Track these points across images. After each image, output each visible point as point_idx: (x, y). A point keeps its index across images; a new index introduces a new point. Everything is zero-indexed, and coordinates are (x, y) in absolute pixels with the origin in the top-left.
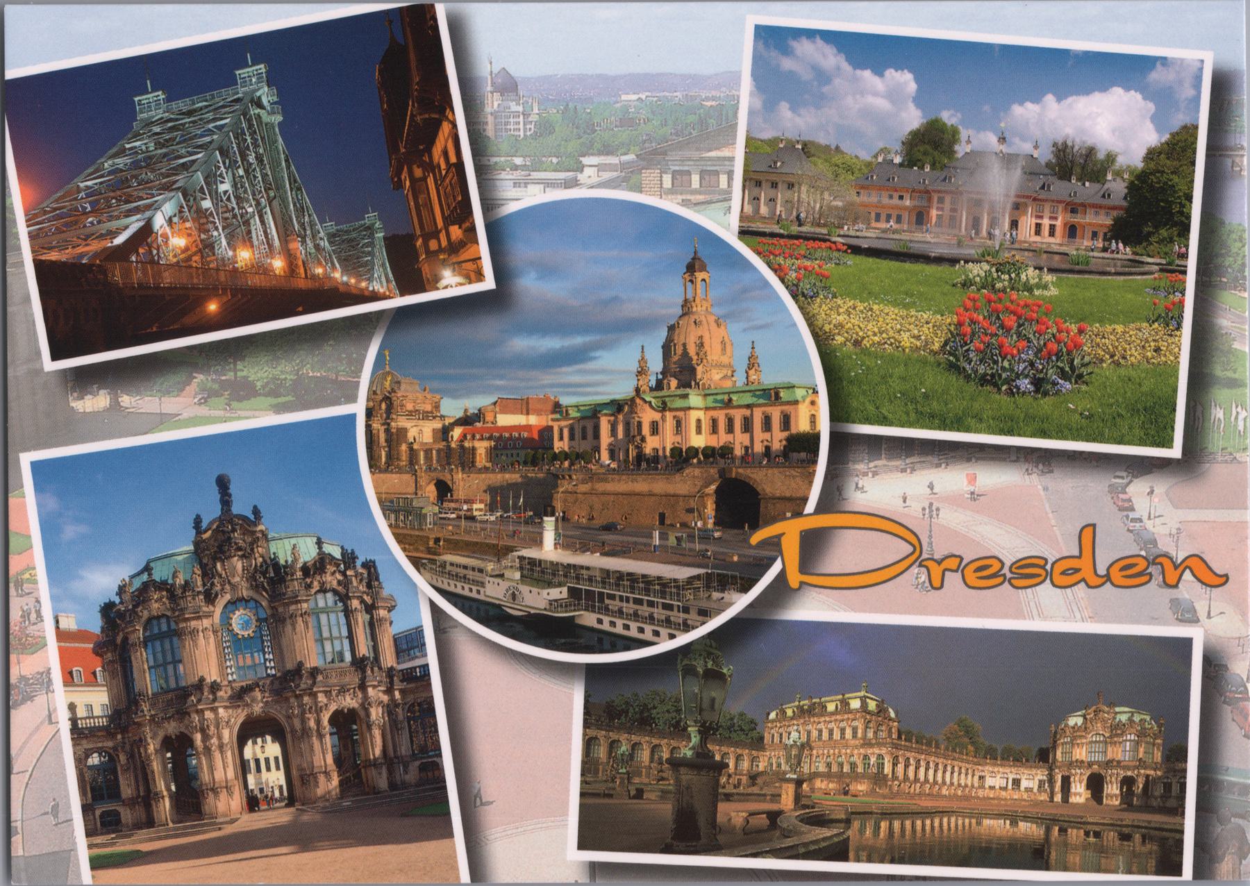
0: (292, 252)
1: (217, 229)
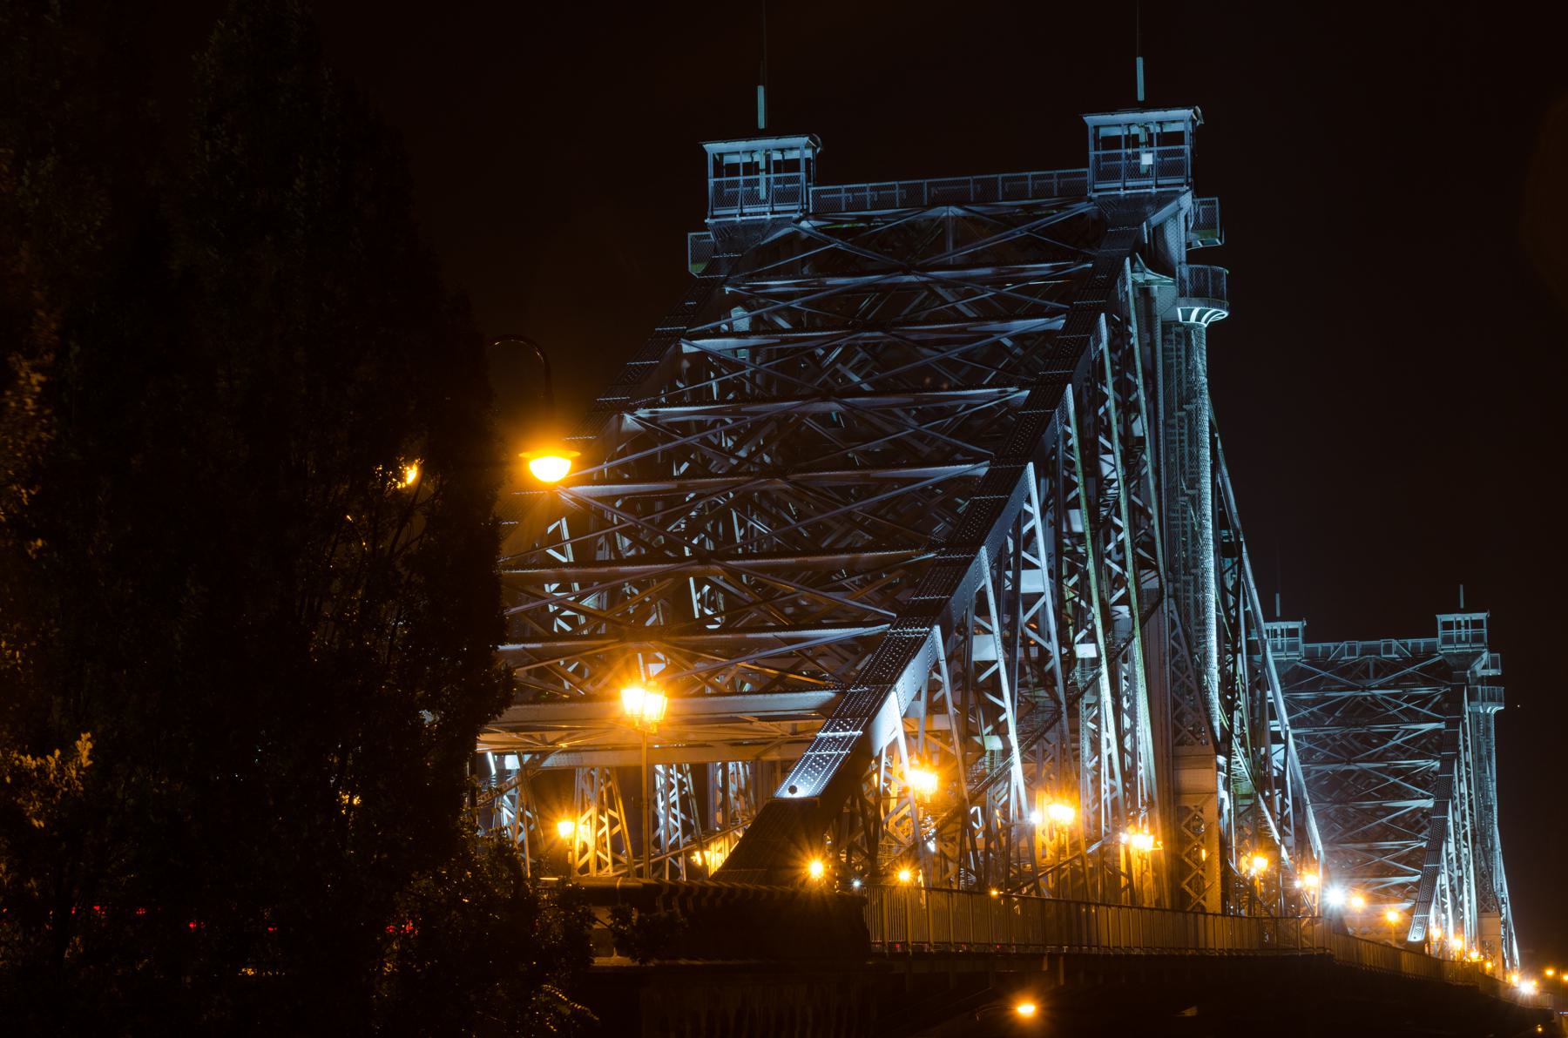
0: (1189, 802)
1: (1001, 730)
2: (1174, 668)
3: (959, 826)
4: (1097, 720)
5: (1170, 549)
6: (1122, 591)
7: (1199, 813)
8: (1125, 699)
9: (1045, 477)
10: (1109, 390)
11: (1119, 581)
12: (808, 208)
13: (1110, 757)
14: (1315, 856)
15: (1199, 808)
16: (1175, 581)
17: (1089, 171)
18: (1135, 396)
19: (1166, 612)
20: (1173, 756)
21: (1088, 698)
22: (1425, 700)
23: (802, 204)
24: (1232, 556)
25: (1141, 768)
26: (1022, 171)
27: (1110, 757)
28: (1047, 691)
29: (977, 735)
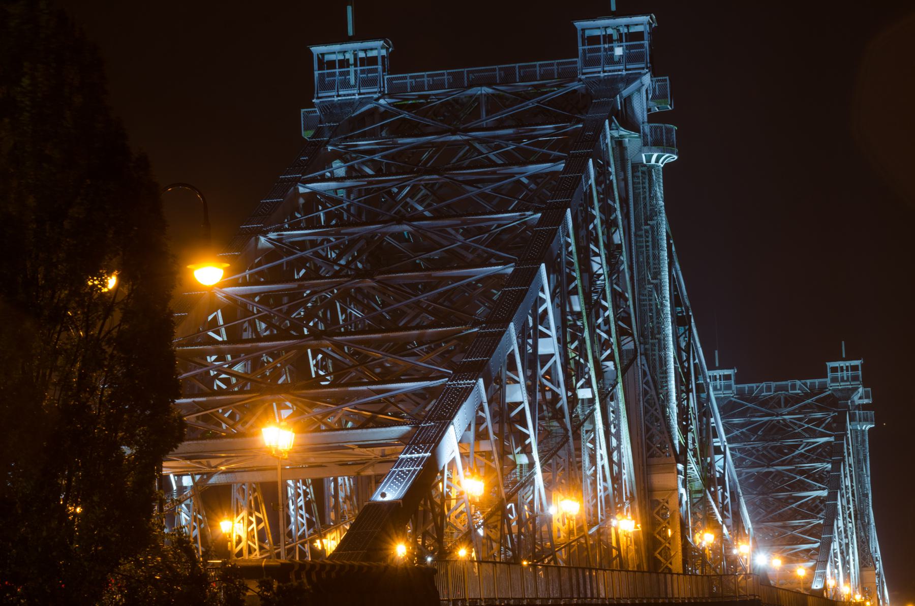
0: (658, 497)
1: (527, 450)
2: (645, 404)
3: (500, 518)
4: (593, 441)
5: (642, 321)
6: (609, 352)
7: (666, 504)
8: (612, 426)
9: (554, 273)
10: (596, 212)
11: (606, 344)
12: (384, 91)
13: (603, 467)
14: (747, 532)
15: (665, 501)
16: (645, 343)
17: (579, 60)
18: (614, 216)
19: (639, 365)
20: (647, 465)
21: (587, 426)
22: (820, 422)
23: (380, 88)
24: (684, 325)
25: (624, 474)
26: (532, 61)
27: (603, 467)
28: (559, 423)
29: (511, 454)
